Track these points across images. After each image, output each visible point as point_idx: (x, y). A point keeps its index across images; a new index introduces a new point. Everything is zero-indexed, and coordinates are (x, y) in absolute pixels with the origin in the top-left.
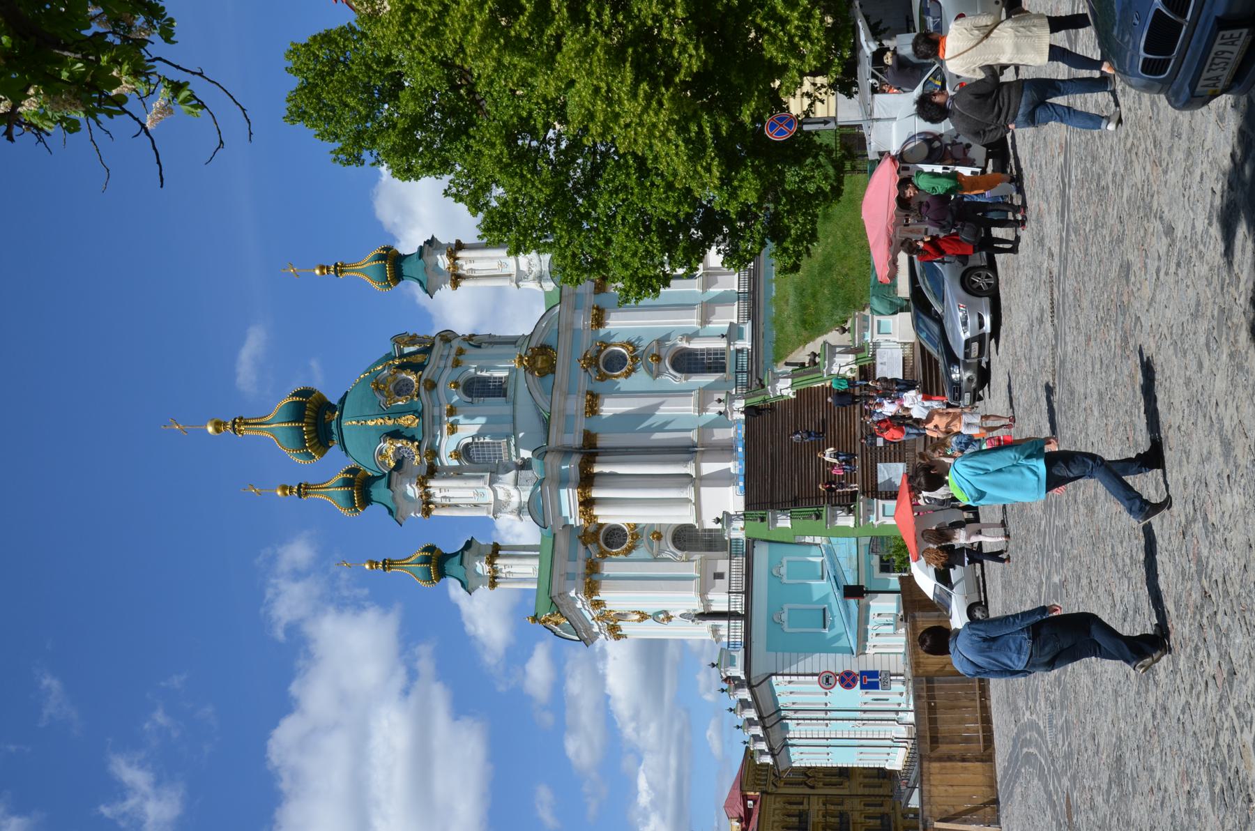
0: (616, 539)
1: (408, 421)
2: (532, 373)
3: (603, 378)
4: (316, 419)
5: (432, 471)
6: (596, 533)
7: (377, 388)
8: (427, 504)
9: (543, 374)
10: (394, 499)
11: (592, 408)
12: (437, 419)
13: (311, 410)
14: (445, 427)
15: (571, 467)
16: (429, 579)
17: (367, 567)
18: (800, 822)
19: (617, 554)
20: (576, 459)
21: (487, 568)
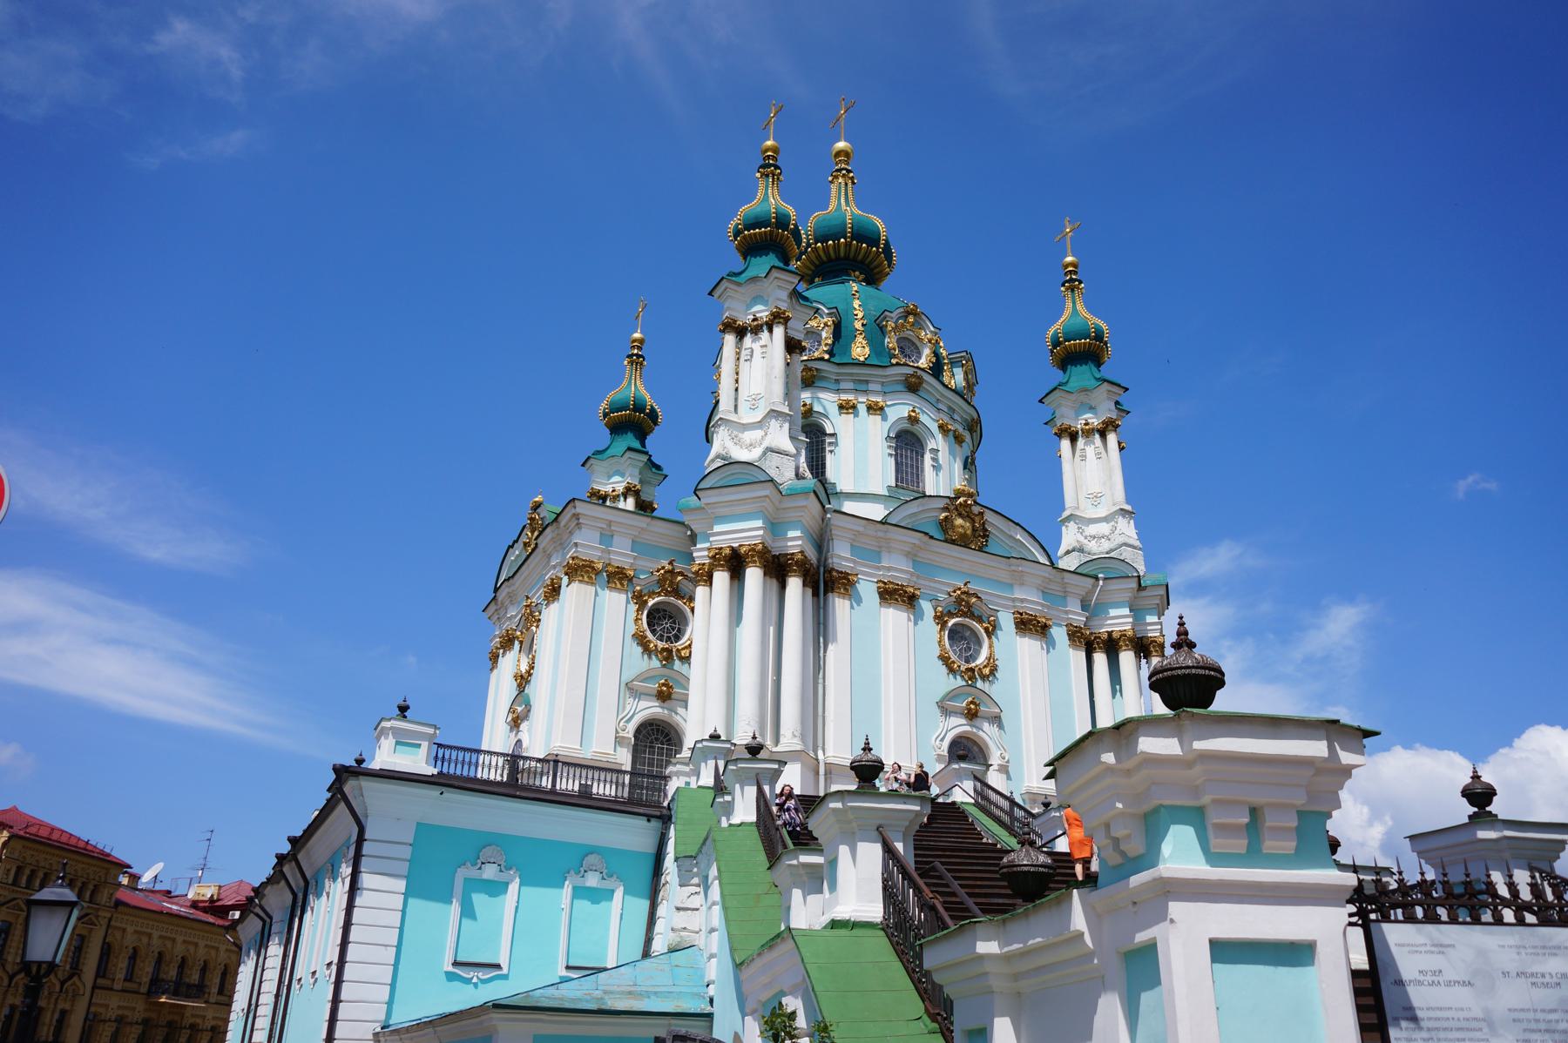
0: (667, 624)
1: (860, 350)
2: (946, 509)
3: (940, 619)
4: (855, 260)
5: (792, 346)
6: (677, 592)
7: (908, 313)
8: (741, 332)
9: (945, 525)
10: (754, 279)
11: (890, 594)
12: (863, 387)
13: (868, 252)
14: (850, 397)
15: (795, 541)
16: (615, 407)
17: (637, 335)
18: (189, 986)
19: (637, 620)
20: (812, 555)
21: (620, 488)
